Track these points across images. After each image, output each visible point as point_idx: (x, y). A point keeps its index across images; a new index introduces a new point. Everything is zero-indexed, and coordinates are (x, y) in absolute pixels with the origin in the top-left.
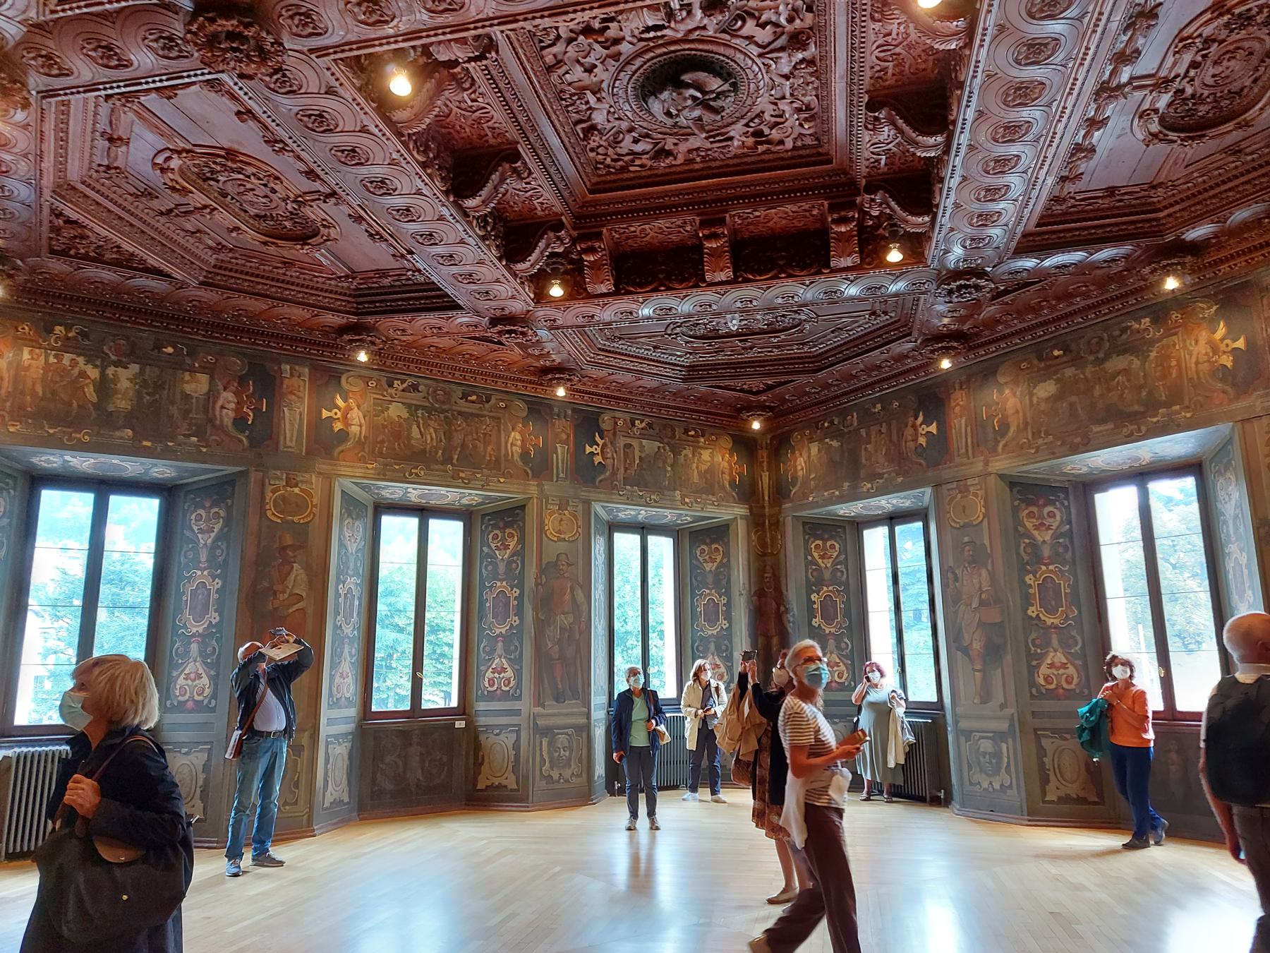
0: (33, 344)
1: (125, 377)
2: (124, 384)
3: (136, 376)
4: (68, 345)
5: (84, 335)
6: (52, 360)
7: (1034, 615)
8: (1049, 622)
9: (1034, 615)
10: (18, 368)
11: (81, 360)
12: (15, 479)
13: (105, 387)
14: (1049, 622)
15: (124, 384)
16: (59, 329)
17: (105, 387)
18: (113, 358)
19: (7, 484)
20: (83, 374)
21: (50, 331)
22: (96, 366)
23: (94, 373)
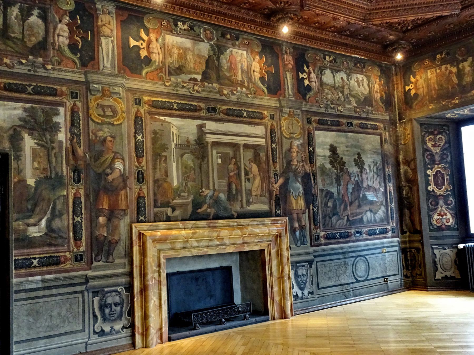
0: (430, 67)
1: (466, 66)
2: (468, 69)
3: (472, 63)
4: (444, 61)
5: (447, 54)
6: (438, 71)
7: (431, 190)
8: (438, 193)
9: (431, 190)
10: (427, 80)
11: (448, 66)
12: (448, 126)
13: (460, 75)
14: (438, 193)
15: (468, 69)
16: (438, 56)
17: (460, 75)
18: (461, 58)
19: (444, 129)
20: (451, 72)
21: (435, 58)
22: (455, 66)
23: (454, 70)
